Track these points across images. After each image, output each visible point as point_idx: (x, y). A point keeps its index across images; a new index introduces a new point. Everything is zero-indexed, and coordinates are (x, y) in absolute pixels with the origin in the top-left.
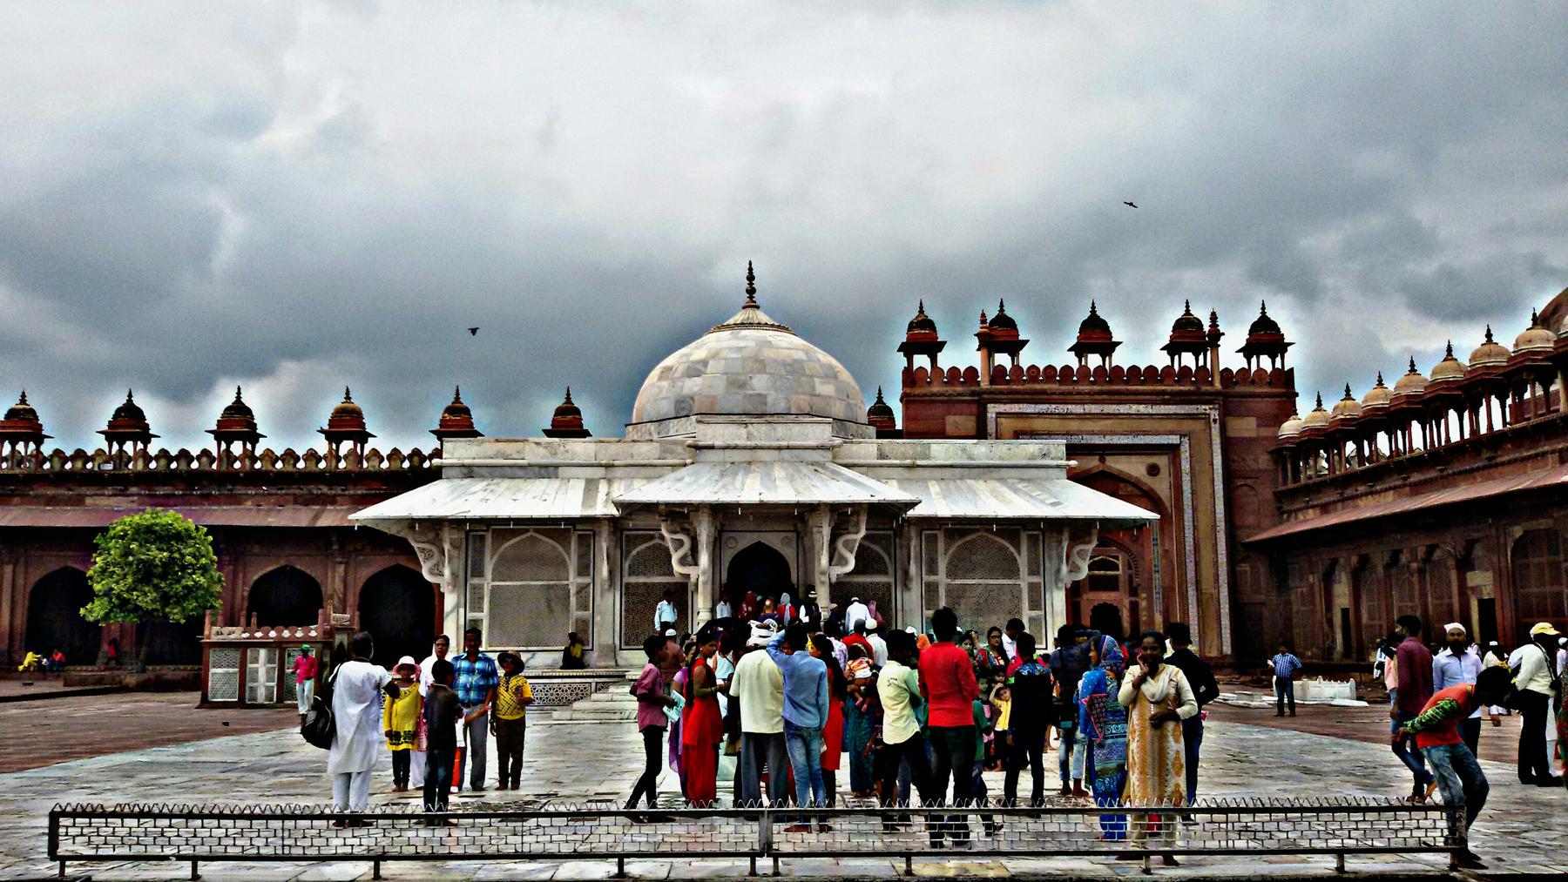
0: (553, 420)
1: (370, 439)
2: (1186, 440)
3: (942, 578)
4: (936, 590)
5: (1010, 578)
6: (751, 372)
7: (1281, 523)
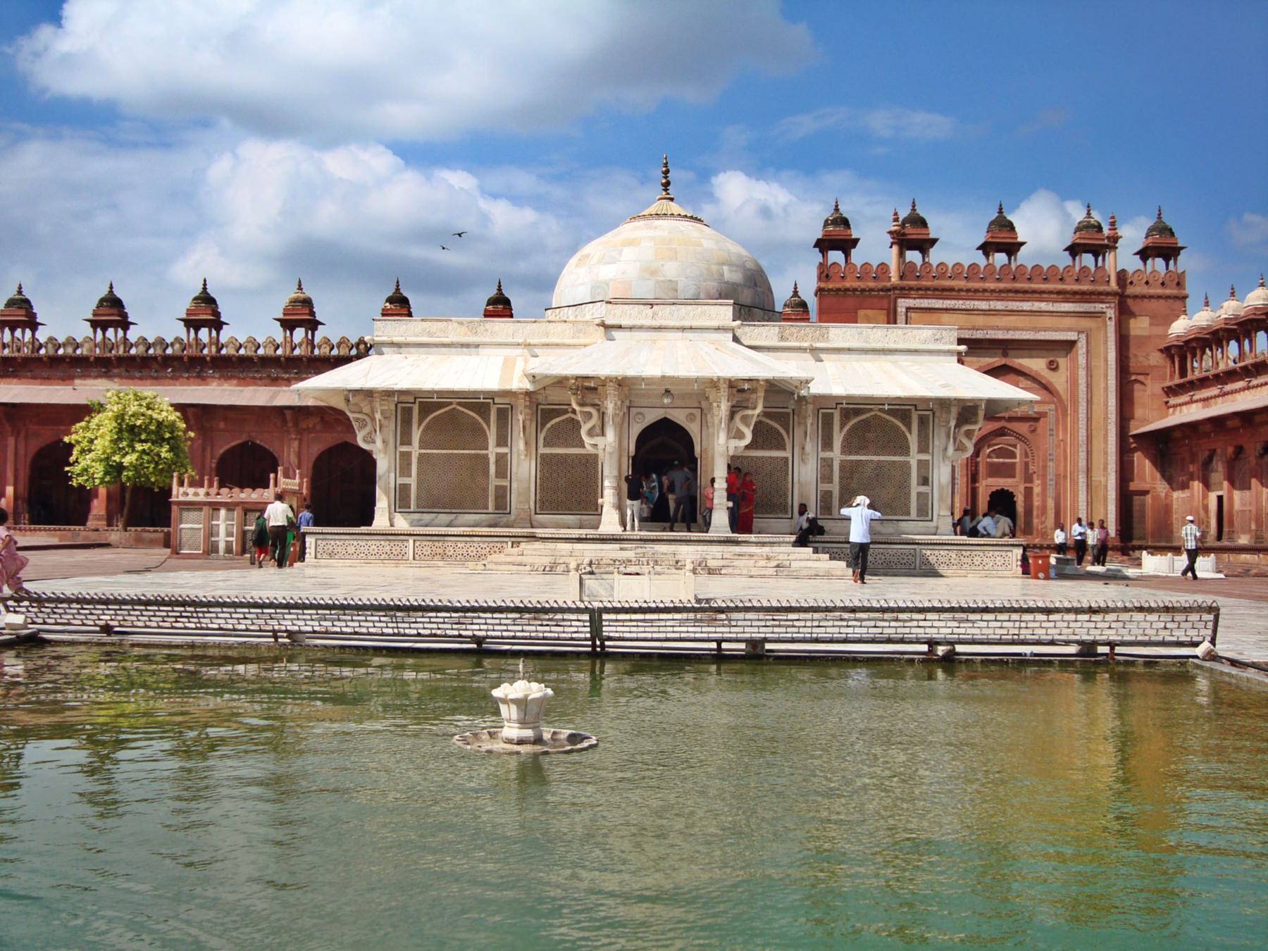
0: (486, 310)
1: (320, 327)
2: (1083, 337)
3: (836, 454)
4: (831, 466)
5: (901, 454)
6: (662, 259)
7: (1167, 416)
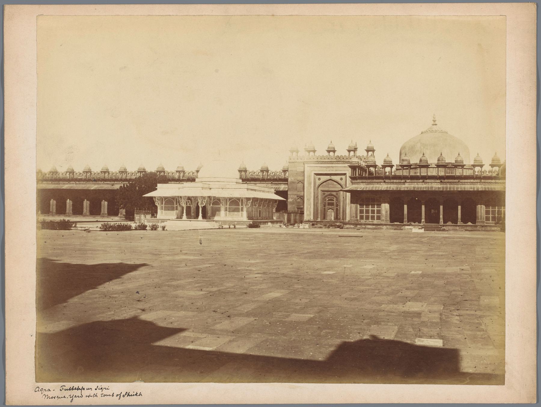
3: (228, 206)
4: (227, 208)
